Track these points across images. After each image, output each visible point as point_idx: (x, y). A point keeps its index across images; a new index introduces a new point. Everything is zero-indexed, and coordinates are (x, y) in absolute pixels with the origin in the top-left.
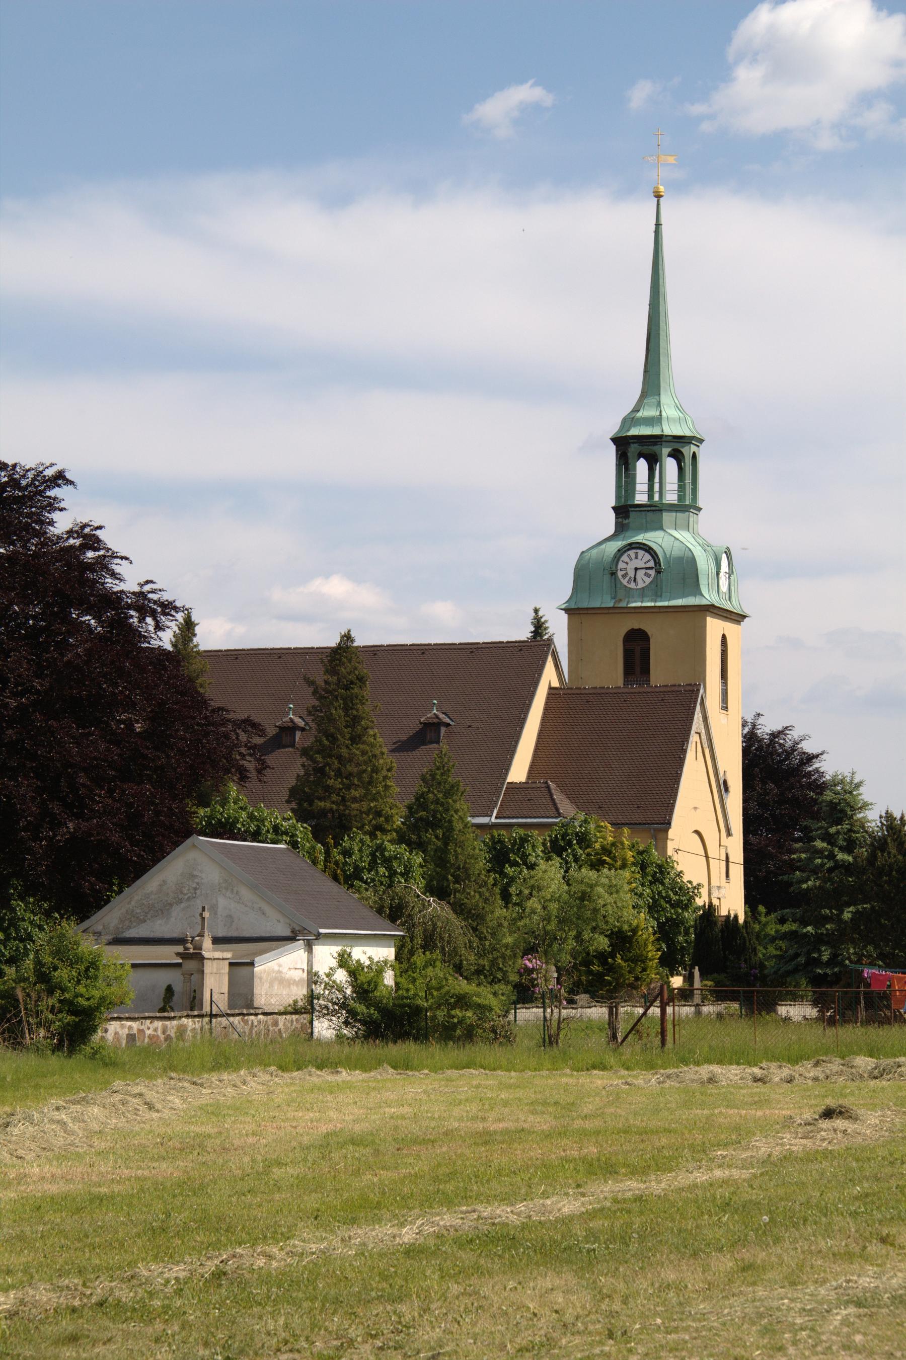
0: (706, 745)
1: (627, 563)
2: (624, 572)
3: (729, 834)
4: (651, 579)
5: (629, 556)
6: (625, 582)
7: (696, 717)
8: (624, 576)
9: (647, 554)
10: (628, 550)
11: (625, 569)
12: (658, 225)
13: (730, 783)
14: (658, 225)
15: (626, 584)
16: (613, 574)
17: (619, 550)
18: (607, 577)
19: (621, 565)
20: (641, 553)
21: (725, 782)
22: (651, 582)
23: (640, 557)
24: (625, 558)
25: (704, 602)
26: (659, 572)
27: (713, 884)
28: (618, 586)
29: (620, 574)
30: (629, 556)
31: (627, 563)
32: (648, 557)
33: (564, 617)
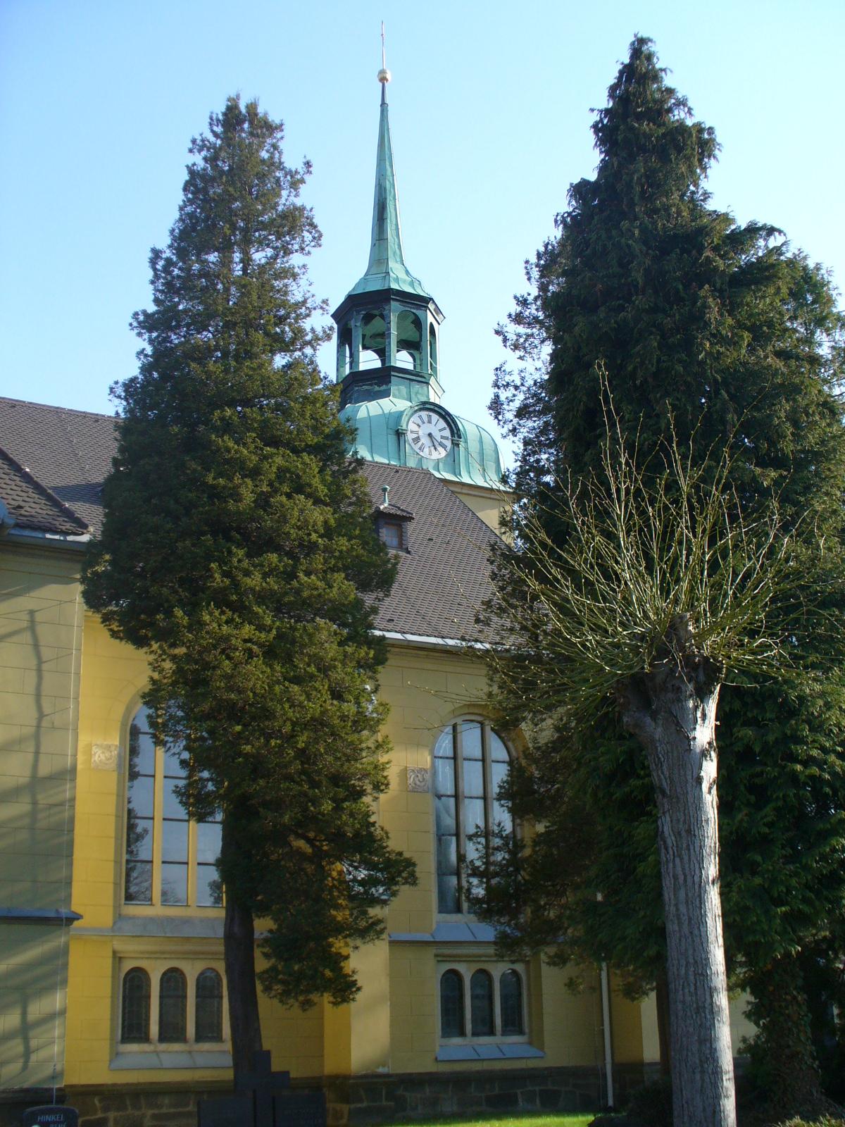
1: (419, 426)
9: (441, 421)
12: (383, 104)
14: (383, 104)
15: (418, 451)
20: (435, 417)
23: (434, 421)
32: (442, 424)
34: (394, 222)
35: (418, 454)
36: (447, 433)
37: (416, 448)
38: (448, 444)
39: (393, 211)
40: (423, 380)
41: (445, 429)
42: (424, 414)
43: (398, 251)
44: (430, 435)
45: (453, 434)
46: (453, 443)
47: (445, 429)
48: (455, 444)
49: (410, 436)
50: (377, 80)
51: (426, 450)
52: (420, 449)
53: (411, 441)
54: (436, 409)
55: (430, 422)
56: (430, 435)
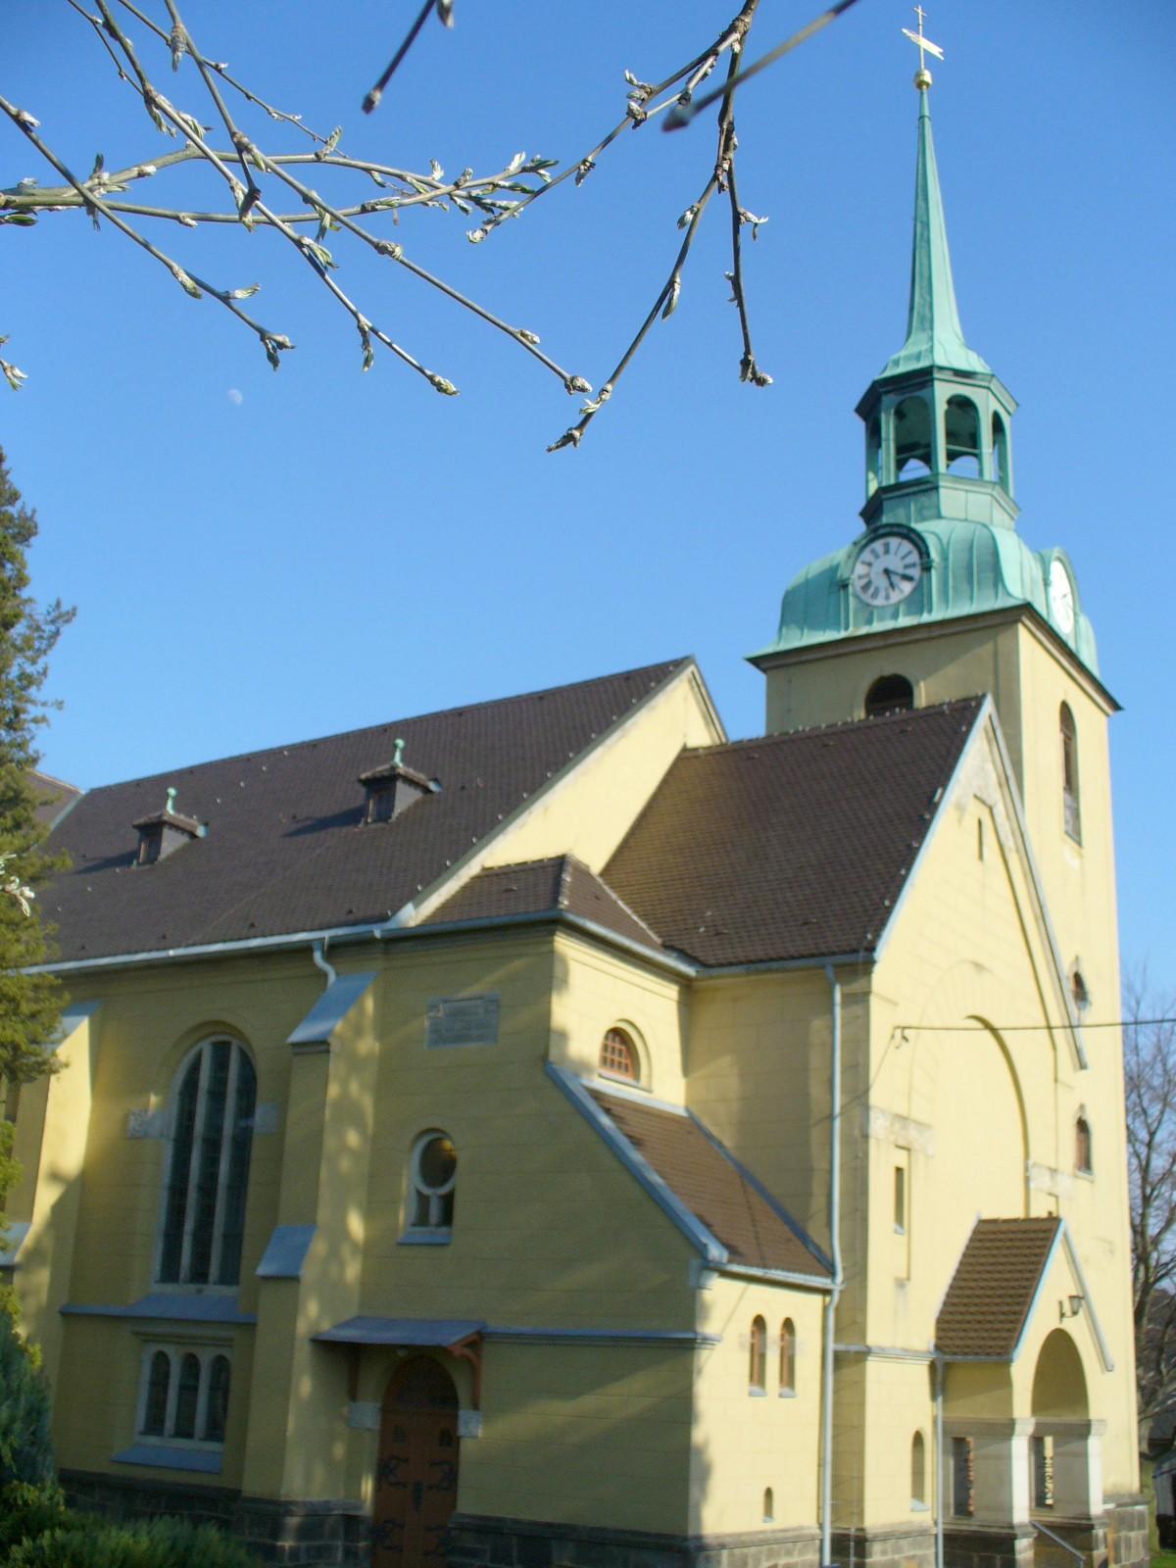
1: (870, 564)
2: (864, 581)
3: (1083, 1066)
5: (873, 551)
10: (872, 540)
13: (1090, 984)
15: (870, 601)
20: (894, 542)
21: (1078, 980)
23: (893, 548)
25: (1010, 603)
27: (1034, 1157)
30: (873, 551)
31: (870, 564)
32: (907, 546)
33: (759, 679)
34: (926, 275)
35: (868, 605)
36: (915, 557)
37: (866, 598)
38: (915, 572)
39: (925, 261)
40: (929, 486)
41: (910, 553)
42: (878, 545)
43: (928, 314)
44: (887, 572)
45: (921, 557)
47: (910, 553)
48: (927, 568)
49: (856, 585)
50: (914, 85)
51: (882, 593)
53: (858, 589)
55: (887, 551)
56: (887, 572)
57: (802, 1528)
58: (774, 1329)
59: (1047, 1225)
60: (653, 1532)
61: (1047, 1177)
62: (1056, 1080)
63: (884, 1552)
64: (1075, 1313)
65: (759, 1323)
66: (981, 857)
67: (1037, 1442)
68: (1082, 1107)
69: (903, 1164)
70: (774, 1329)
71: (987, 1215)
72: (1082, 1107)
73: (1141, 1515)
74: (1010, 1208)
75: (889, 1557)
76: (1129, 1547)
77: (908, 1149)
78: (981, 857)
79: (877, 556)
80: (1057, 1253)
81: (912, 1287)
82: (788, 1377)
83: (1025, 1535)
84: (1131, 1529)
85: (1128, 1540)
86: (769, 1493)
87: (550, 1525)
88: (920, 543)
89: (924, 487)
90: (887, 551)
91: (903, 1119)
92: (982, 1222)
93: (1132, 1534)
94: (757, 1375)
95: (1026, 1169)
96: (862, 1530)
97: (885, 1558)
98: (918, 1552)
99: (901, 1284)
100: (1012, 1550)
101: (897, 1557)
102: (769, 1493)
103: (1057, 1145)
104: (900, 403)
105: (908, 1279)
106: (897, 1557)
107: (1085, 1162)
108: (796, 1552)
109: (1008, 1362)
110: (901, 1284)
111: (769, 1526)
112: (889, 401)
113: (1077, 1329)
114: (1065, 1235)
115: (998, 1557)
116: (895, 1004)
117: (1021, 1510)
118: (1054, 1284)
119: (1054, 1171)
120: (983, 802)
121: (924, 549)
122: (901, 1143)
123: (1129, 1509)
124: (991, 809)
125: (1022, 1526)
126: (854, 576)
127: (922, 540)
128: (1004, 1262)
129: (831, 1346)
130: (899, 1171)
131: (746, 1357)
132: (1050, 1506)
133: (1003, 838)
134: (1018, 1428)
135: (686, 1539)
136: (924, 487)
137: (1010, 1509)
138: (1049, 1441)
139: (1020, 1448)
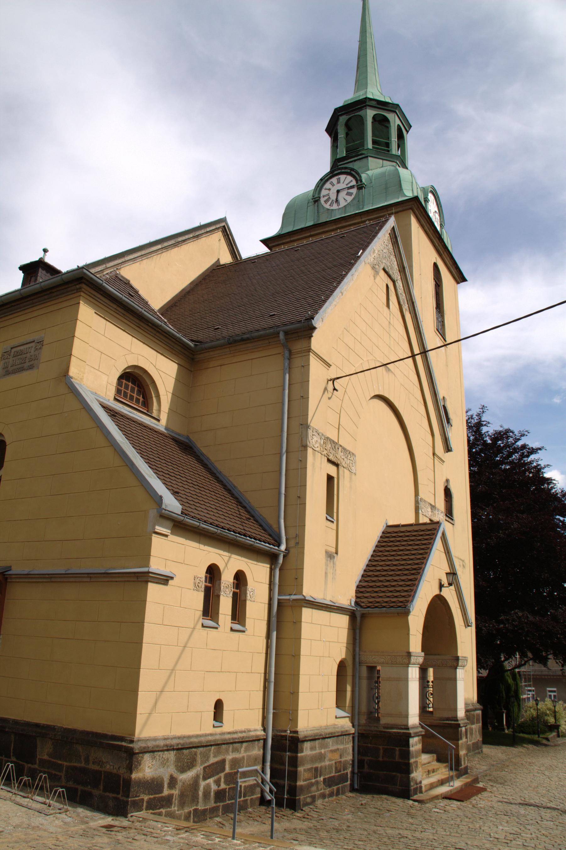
0: (405, 307)
3: (448, 449)
4: (353, 196)
6: (327, 206)
7: (380, 235)
8: (326, 202)
10: (331, 178)
11: (328, 195)
16: (316, 200)
17: (321, 180)
18: (311, 208)
19: (324, 192)
20: (342, 177)
22: (354, 199)
23: (342, 181)
24: (328, 185)
26: (360, 187)
27: (421, 495)
28: (321, 210)
29: (322, 200)
31: (329, 189)
32: (349, 178)
40: (363, 156)
41: (352, 181)
42: (334, 180)
46: (358, 189)
47: (352, 181)
52: (330, 205)
54: (343, 171)
55: (339, 182)
57: (249, 731)
58: (227, 578)
59: (429, 527)
60: (110, 734)
61: (429, 510)
62: (434, 454)
63: (312, 749)
64: (450, 584)
65: (213, 572)
66: (388, 306)
67: (423, 671)
68: (447, 481)
69: (334, 474)
70: (227, 578)
71: (391, 523)
72: (447, 481)
73: (478, 715)
74: (405, 517)
75: (318, 751)
76: (471, 734)
77: (337, 465)
78: (388, 306)
79: (333, 185)
80: (438, 544)
81: (339, 559)
82: (238, 614)
83: (416, 735)
84: (473, 723)
85: (471, 729)
86: (219, 705)
87: (37, 725)
88: (356, 176)
89: (360, 157)
90: (339, 182)
91: (335, 444)
92: (388, 526)
93: (473, 726)
94: (210, 609)
95: (417, 502)
96: (296, 732)
97: (314, 752)
98: (341, 747)
99: (331, 556)
100: (407, 745)
101: (323, 751)
102: (219, 705)
103: (433, 496)
104: (349, 120)
105: (337, 553)
106: (323, 751)
107: (449, 513)
108: (243, 749)
109: (407, 613)
110: (331, 556)
111: (218, 730)
112: (343, 119)
113: (449, 594)
114: (443, 534)
115: (397, 749)
116: (329, 365)
117: (414, 718)
118: (435, 569)
119: (433, 507)
120: (389, 276)
121: (359, 179)
122: (331, 458)
123: (473, 713)
124: (394, 282)
125: (414, 727)
126: (322, 195)
127: (358, 174)
128: (401, 553)
129: (276, 597)
130: (330, 479)
131: (200, 597)
132: (431, 712)
133: (402, 303)
134: (413, 660)
135: (132, 741)
136: (360, 157)
137: (407, 716)
138: (431, 671)
139: (414, 673)
